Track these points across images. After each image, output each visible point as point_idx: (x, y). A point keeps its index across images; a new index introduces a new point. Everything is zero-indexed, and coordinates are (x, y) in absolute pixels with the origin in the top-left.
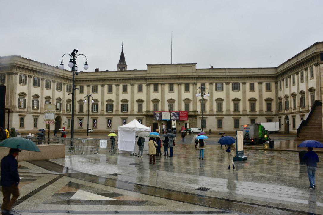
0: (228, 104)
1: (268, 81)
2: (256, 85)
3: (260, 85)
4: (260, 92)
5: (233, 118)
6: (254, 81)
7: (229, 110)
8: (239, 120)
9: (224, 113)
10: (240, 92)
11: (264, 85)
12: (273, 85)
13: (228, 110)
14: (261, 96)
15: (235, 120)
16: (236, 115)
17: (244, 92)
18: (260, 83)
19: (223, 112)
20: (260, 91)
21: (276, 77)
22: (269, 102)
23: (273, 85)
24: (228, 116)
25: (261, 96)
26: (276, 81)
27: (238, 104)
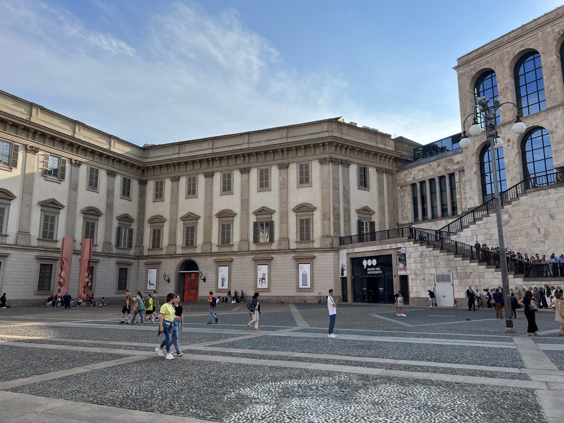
0: (25, 217)
1: (128, 174)
2: (103, 176)
3: (111, 179)
4: (108, 195)
5: (38, 258)
6: (101, 165)
7: (28, 233)
8: (95, 268)
9: (10, 240)
10: (62, 183)
11: (118, 180)
12: (135, 186)
13: (23, 233)
14: (110, 206)
15: (41, 264)
16: (46, 250)
17: (74, 188)
18: (111, 174)
19: (7, 236)
20: (110, 193)
21: (143, 171)
22: (190, 223)
23: (135, 186)
24: (20, 252)
25: (110, 206)
26: (141, 178)
27: (53, 219)
